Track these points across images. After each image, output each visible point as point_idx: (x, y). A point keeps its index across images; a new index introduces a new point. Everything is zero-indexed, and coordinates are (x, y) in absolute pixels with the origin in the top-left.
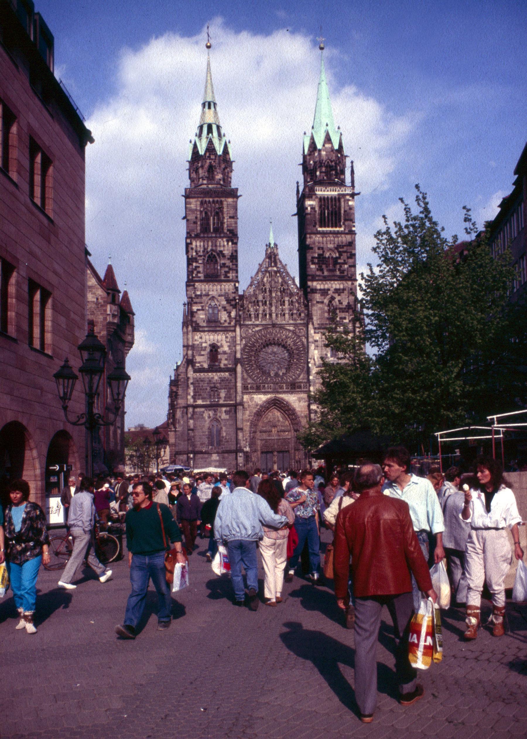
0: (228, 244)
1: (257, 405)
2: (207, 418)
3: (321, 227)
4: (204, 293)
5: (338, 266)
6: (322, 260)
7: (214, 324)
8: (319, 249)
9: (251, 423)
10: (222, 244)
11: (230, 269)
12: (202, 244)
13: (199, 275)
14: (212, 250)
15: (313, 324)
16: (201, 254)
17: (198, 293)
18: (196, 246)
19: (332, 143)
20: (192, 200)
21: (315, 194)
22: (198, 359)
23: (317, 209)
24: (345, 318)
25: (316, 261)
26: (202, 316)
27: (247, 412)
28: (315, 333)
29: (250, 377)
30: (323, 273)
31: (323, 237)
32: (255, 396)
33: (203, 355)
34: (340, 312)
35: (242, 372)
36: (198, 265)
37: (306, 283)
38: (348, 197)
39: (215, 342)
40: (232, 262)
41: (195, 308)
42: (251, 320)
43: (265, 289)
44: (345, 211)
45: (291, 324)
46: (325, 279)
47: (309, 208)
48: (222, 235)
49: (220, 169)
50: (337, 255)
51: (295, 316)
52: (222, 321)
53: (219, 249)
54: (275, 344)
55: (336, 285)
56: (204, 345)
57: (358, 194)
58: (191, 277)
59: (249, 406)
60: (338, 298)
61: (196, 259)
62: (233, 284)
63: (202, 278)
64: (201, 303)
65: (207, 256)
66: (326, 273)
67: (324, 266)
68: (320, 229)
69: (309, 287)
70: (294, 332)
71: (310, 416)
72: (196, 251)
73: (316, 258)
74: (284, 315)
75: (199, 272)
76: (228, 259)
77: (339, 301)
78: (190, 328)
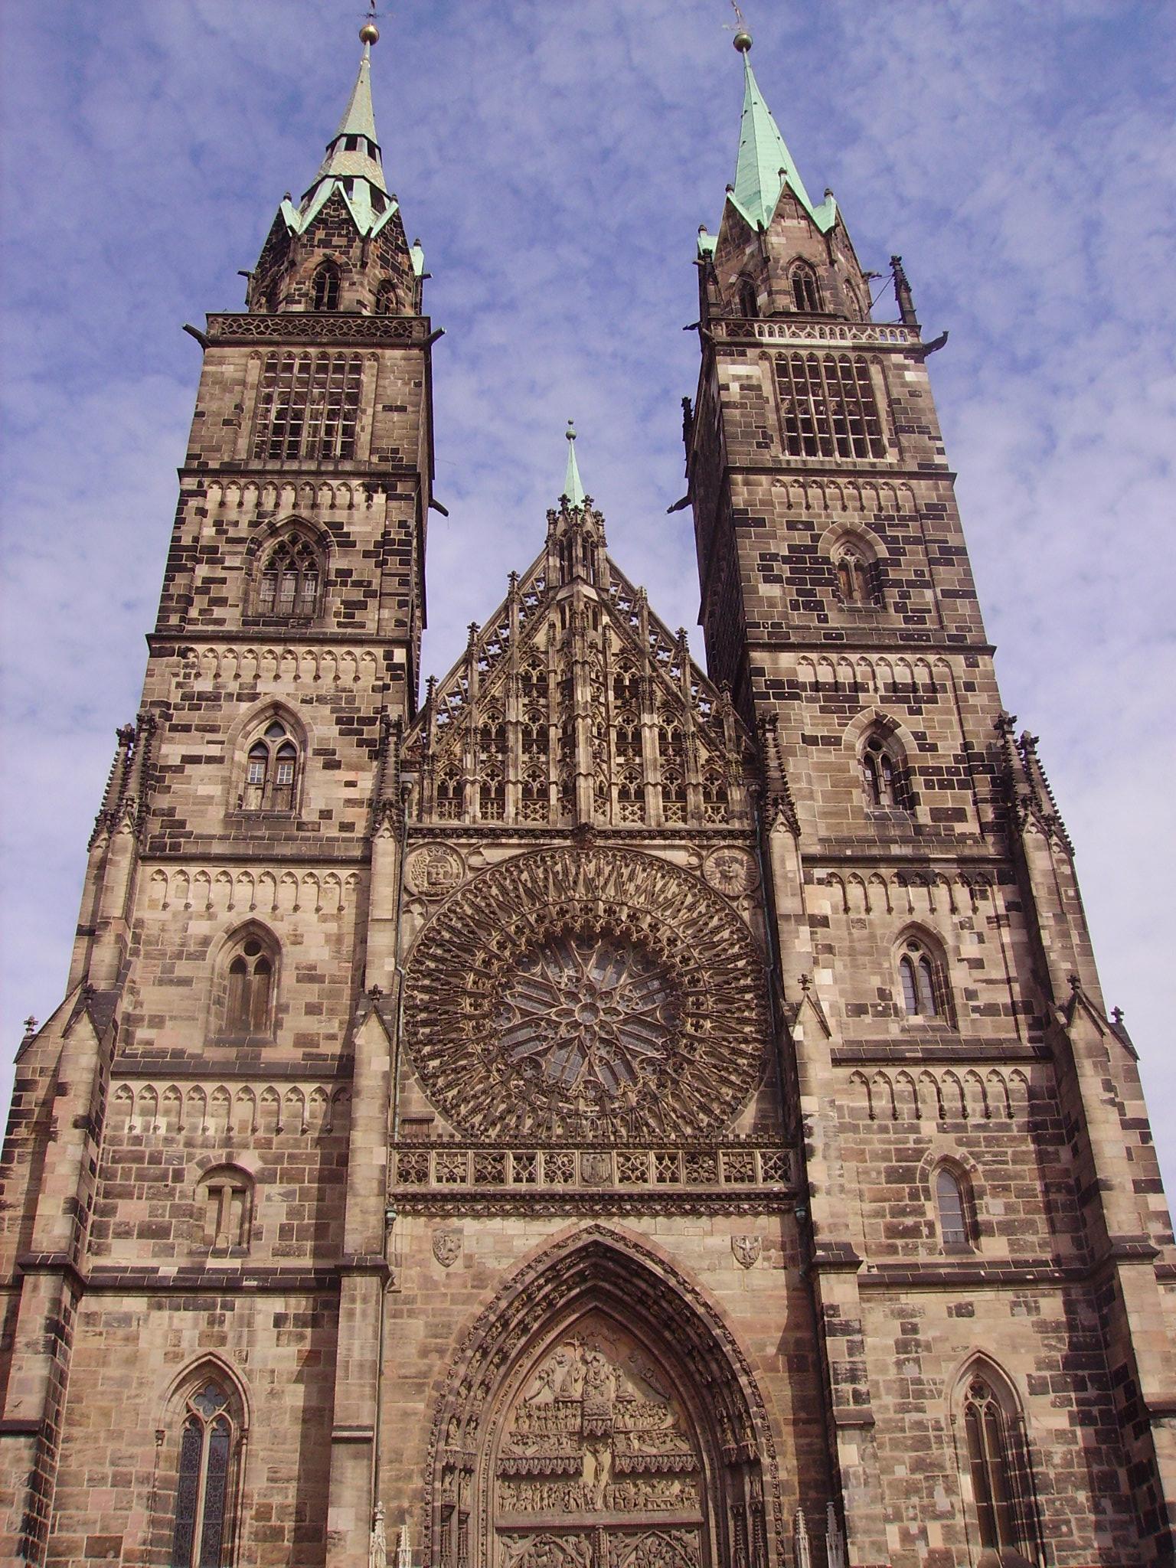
0: (369, 498)
1: (480, 1280)
2: (156, 1359)
3: (795, 452)
4: (233, 687)
5: (892, 595)
6: (806, 568)
7: (268, 839)
8: (791, 526)
9: (439, 1407)
10: (343, 497)
11: (372, 594)
12: (251, 495)
13: (218, 612)
14: (295, 521)
15: (794, 829)
16: (243, 531)
17: (204, 685)
18: (222, 504)
19: (808, 217)
20: (228, 351)
21: (760, 345)
22: (153, 998)
23: (768, 390)
24: (960, 815)
25: (786, 571)
26: (203, 790)
27: (417, 1328)
28: (809, 880)
29: (446, 1112)
30: (824, 619)
31: (803, 486)
32: (469, 1225)
33: (185, 982)
34: (929, 785)
35: (393, 1079)
36: (220, 573)
37: (745, 658)
38: (897, 358)
39: (262, 915)
40: (381, 564)
41: (172, 751)
42: (459, 816)
43: (542, 678)
44: (892, 402)
45: (675, 834)
46: (834, 644)
47: (735, 387)
48: (348, 466)
49: (363, 274)
50: (882, 550)
51: (694, 799)
52: (309, 815)
53: (325, 516)
54: (586, 939)
55: (897, 669)
56: (199, 928)
57: (940, 343)
58: (174, 620)
59: (427, 1281)
60: (907, 727)
61: (214, 550)
62: (379, 652)
63: (229, 627)
64: (213, 729)
65: (270, 545)
66: (836, 621)
67: (824, 594)
68: (787, 456)
69: (761, 672)
70: (693, 878)
71: (821, 1352)
72: (218, 524)
73: (786, 560)
74: (640, 795)
75: (222, 602)
76: (367, 554)
77: (919, 736)
78: (125, 837)
